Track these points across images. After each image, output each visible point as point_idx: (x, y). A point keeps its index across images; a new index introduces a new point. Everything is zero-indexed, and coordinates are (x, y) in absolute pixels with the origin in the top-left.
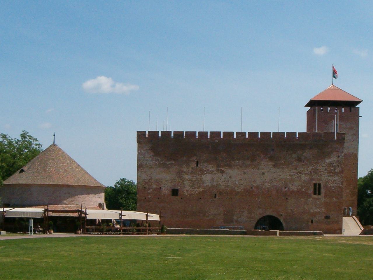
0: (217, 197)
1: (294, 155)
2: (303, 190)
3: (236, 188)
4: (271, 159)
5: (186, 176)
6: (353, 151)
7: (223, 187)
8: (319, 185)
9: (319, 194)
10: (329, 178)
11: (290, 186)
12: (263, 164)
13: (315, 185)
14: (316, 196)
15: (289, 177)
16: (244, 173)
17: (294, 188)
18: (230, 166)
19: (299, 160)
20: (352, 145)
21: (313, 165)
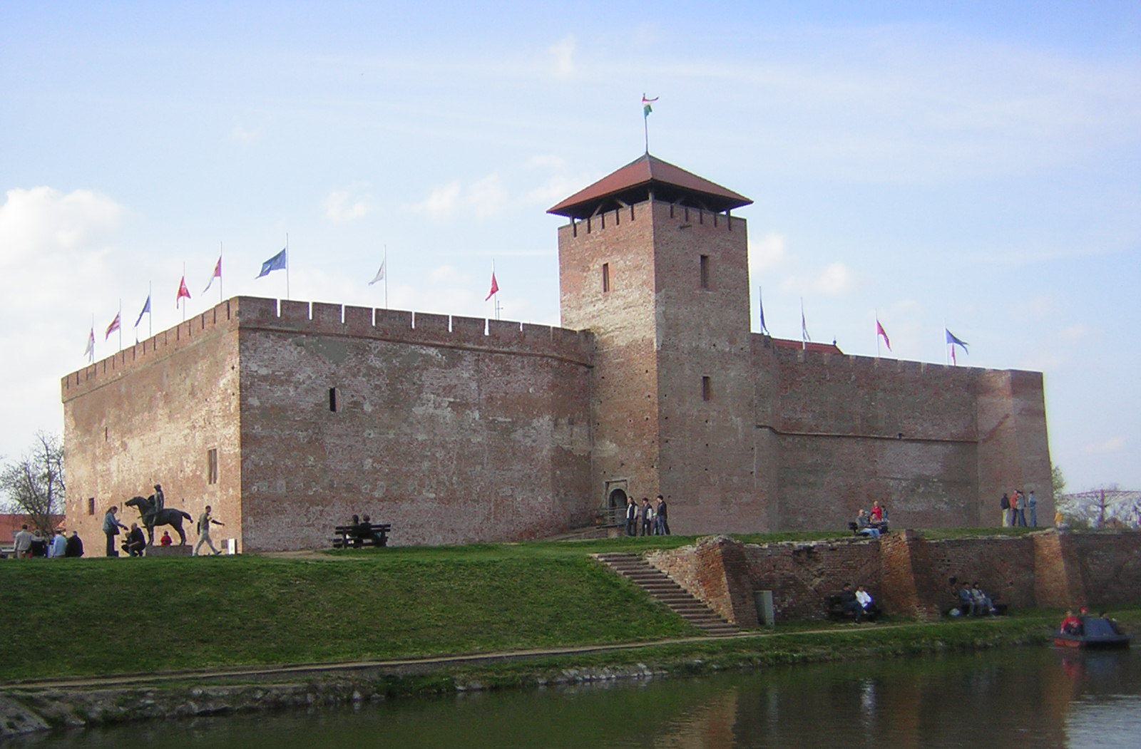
0: (123, 511)
1: (188, 382)
2: (198, 473)
3: (138, 484)
4: (168, 399)
5: (99, 467)
6: (644, 334)
7: (127, 483)
8: (215, 450)
9: (215, 482)
10: (225, 432)
11: (185, 463)
12: (160, 416)
13: (210, 451)
14: (211, 488)
15: (184, 442)
16: (144, 445)
17: (188, 471)
18: (131, 431)
19: (193, 394)
20: (642, 316)
21: (206, 400)
